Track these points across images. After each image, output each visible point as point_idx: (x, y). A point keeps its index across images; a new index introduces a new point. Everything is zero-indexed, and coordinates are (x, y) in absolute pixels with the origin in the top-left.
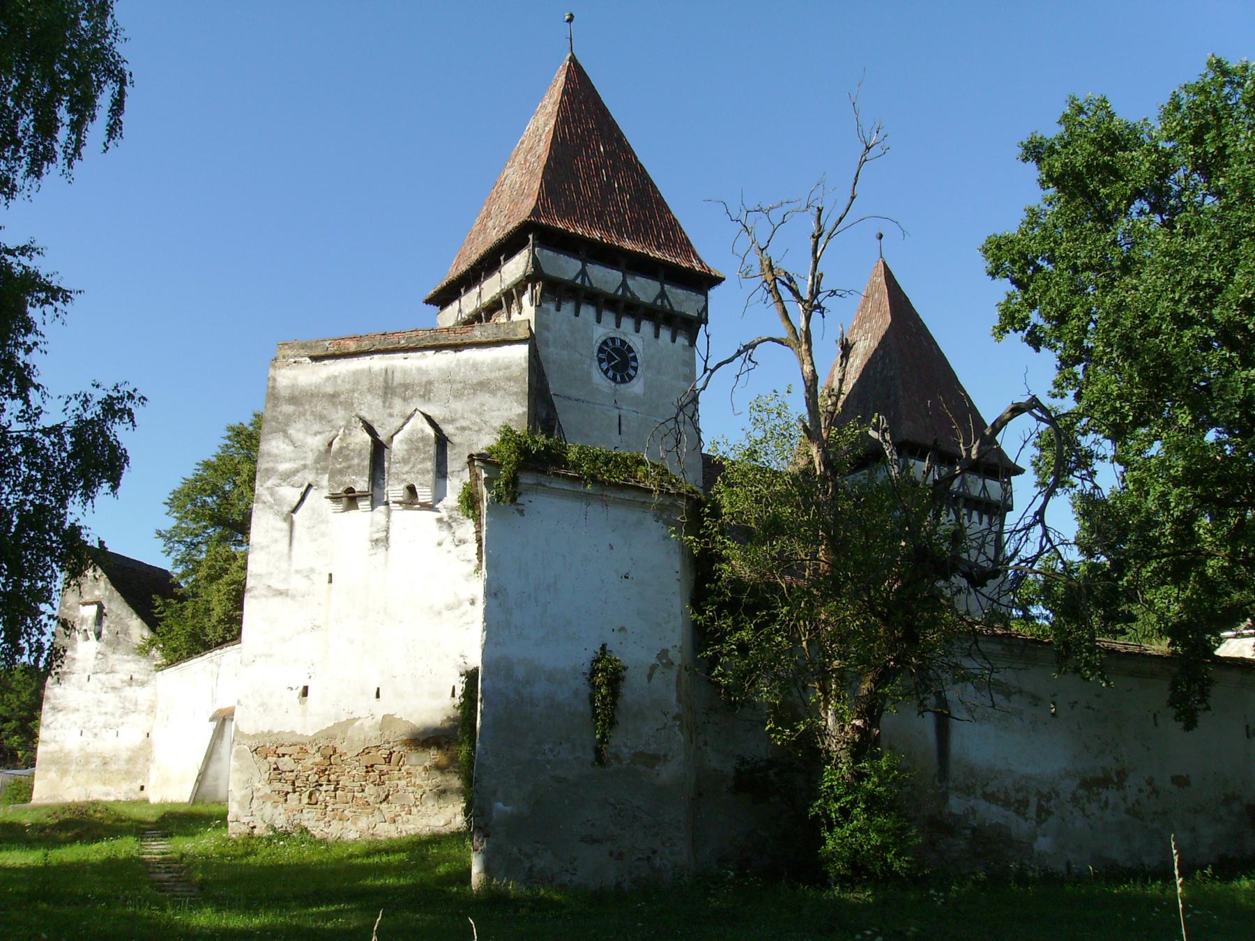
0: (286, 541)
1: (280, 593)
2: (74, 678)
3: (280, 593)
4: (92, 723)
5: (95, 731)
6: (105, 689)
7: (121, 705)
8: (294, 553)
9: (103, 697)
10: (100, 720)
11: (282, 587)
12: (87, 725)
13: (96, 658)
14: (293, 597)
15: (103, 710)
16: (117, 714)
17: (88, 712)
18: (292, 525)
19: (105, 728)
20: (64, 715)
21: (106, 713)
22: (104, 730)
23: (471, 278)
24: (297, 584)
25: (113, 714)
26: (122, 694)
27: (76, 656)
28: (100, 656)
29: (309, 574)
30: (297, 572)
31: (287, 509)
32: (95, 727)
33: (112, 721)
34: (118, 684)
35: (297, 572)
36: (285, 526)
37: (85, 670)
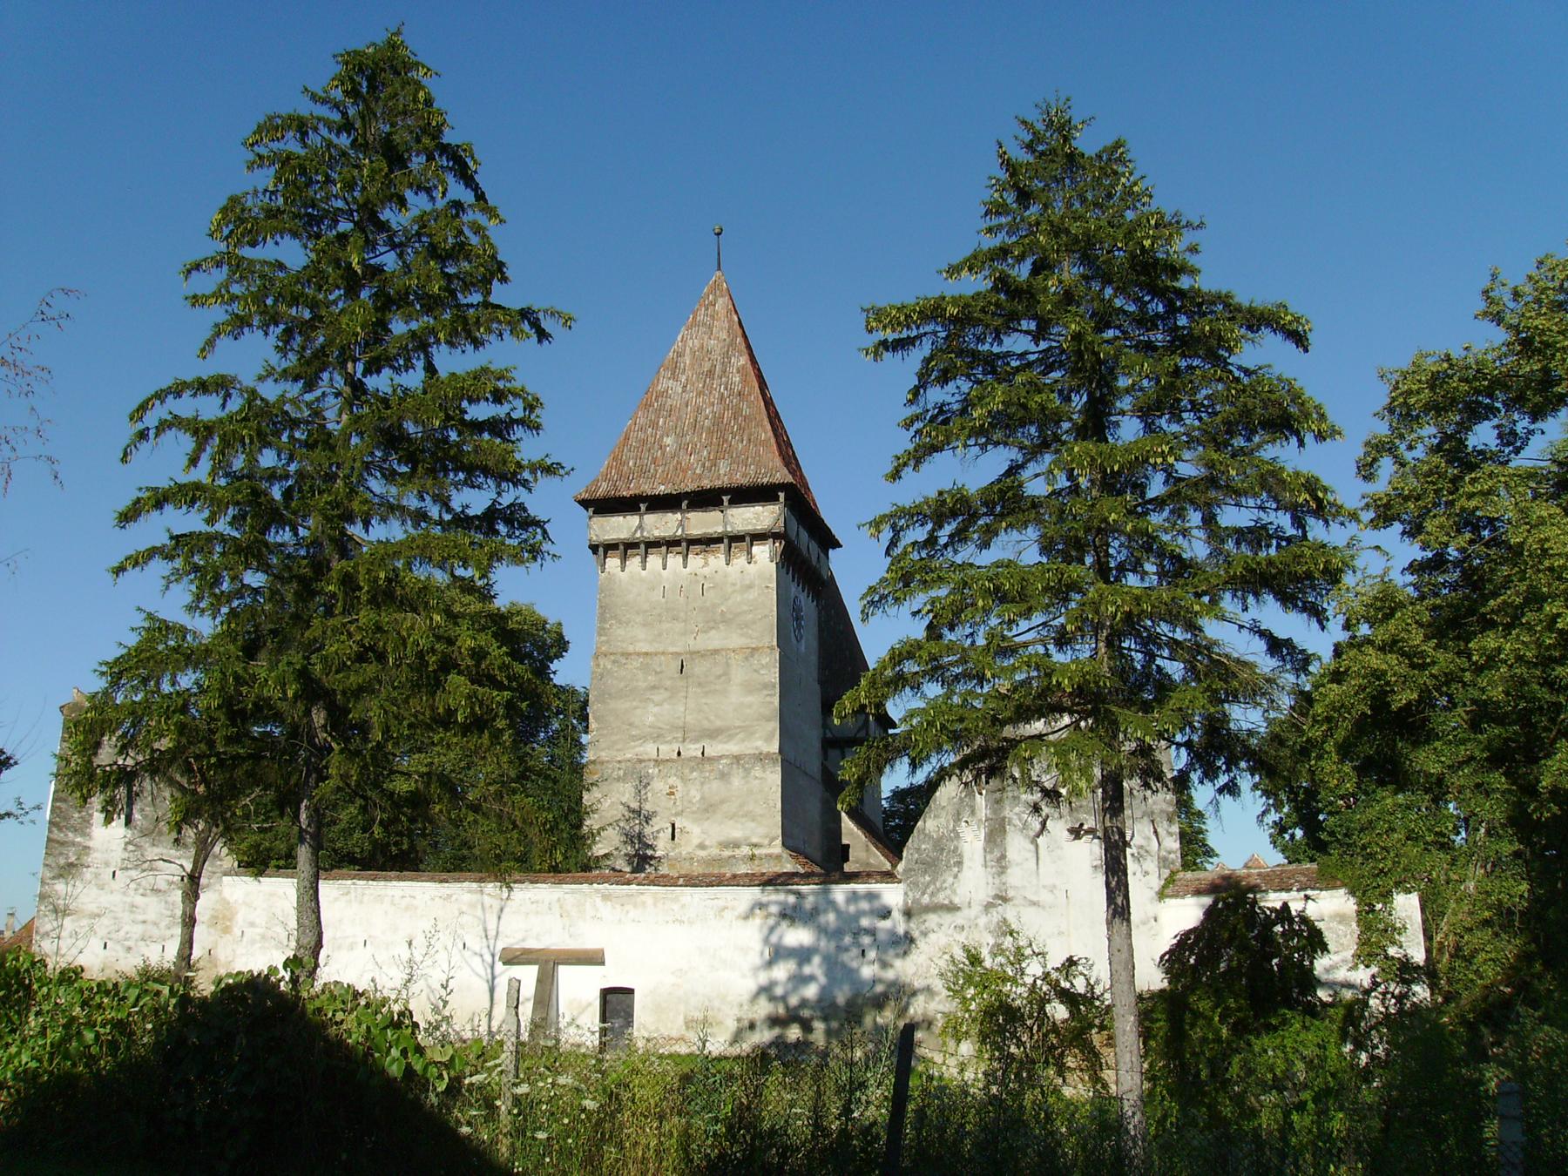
0: (1032, 855)
1: (1034, 904)
2: (88, 874)
3: (1034, 904)
4: (122, 933)
5: (127, 943)
6: (141, 891)
7: (169, 913)
8: (1041, 871)
9: (139, 900)
10: (138, 930)
11: (1035, 898)
12: (113, 936)
13: (125, 849)
14: (1044, 908)
15: (141, 918)
16: (163, 925)
17: (115, 918)
18: (1037, 846)
19: (143, 939)
20: (73, 921)
21: (144, 922)
22: (142, 943)
23: (706, 499)
24: (1044, 897)
25: (155, 924)
26: (169, 899)
27: (91, 844)
28: (131, 847)
29: (1052, 889)
30: (1044, 887)
31: (1032, 834)
32: (126, 940)
33: (155, 932)
34: (162, 885)
35: (1044, 887)
36: (1032, 847)
37: (107, 864)
